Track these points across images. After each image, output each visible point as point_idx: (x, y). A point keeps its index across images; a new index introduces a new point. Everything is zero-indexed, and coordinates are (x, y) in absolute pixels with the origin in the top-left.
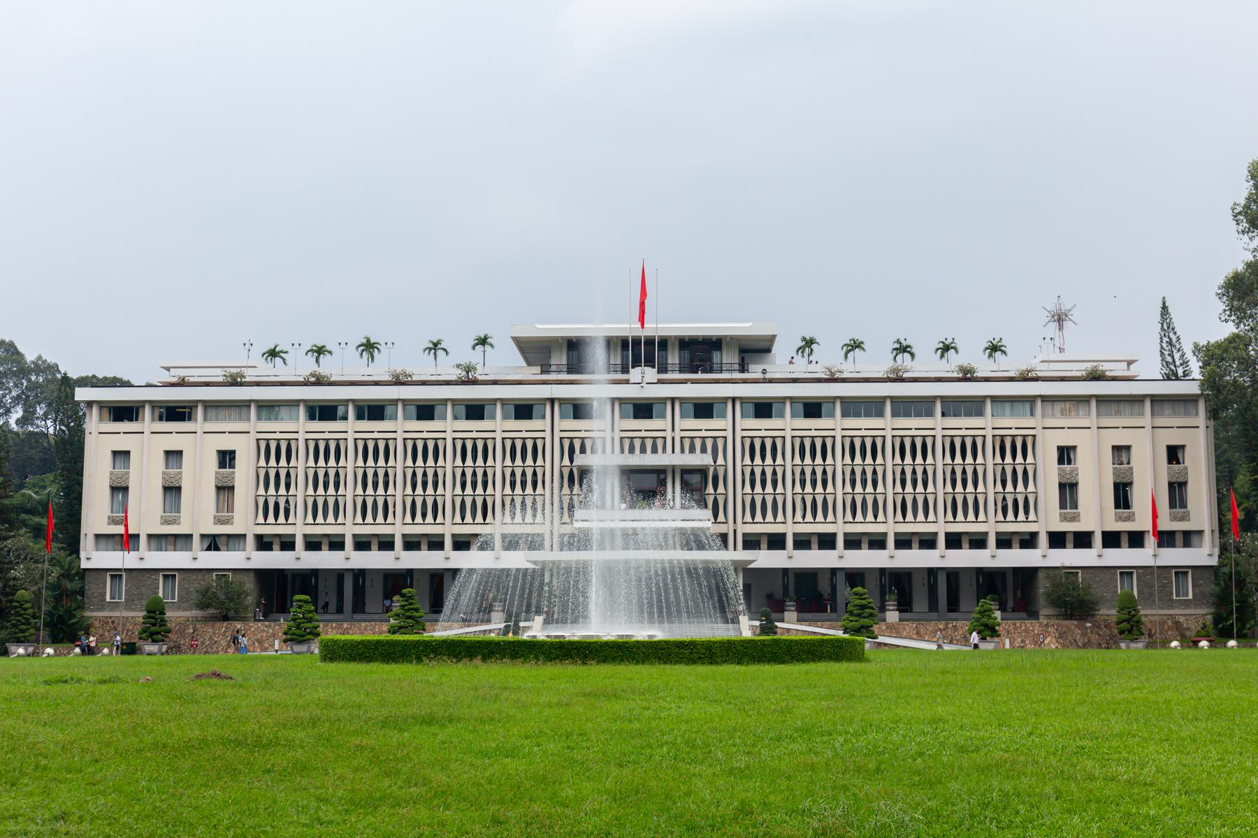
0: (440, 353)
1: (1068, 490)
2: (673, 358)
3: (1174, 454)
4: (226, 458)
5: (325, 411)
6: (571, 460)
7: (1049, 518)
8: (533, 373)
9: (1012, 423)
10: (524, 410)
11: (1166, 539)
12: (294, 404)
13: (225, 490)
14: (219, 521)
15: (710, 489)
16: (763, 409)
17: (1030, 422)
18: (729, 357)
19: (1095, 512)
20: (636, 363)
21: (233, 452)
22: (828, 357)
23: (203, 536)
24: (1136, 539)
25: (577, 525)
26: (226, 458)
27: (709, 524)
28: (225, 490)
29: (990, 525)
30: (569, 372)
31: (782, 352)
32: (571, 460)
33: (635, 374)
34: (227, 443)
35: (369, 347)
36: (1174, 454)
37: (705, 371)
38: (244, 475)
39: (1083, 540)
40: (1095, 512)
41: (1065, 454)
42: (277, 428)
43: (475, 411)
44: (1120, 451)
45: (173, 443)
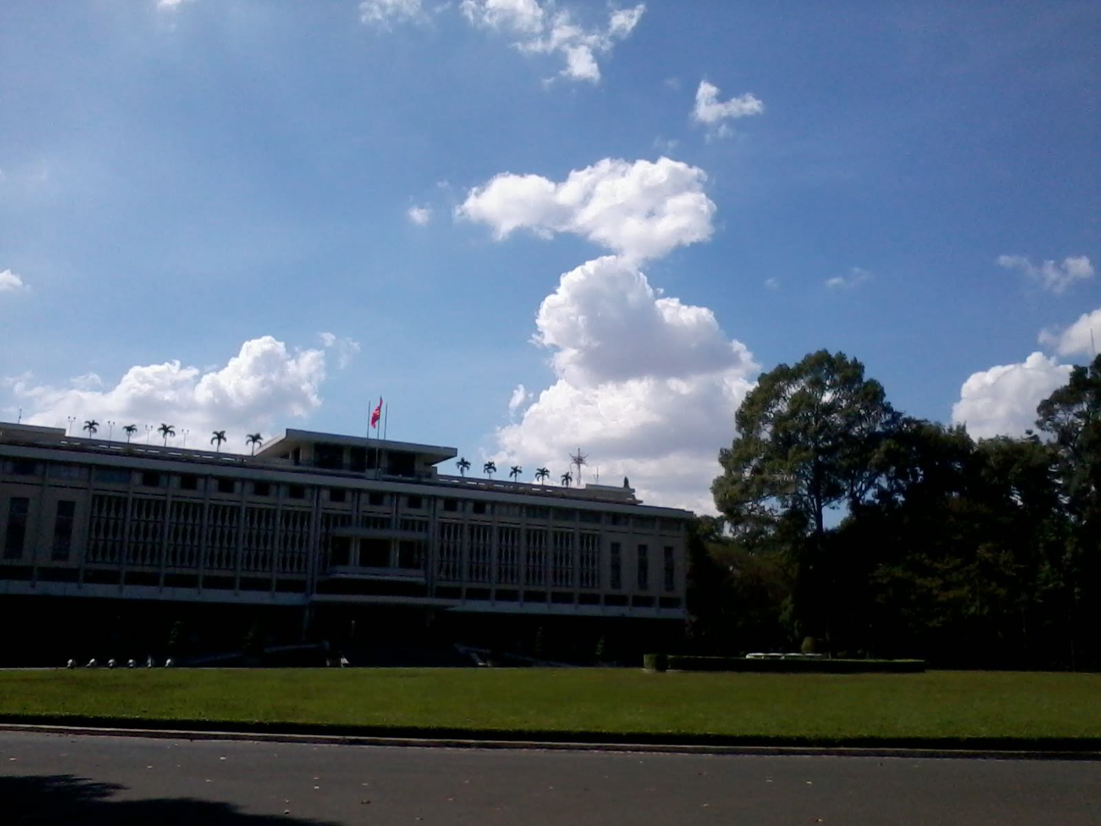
0: (222, 441)
1: (616, 567)
2: (385, 463)
3: (669, 551)
4: (66, 508)
5: (151, 478)
6: (327, 528)
7: (606, 588)
8: (288, 464)
9: (589, 527)
10: (296, 491)
11: (666, 603)
12: (130, 470)
13: (63, 530)
14: (56, 556)
15: (416, 556)
16: (451, 504)
17: (597, 526)
18: (418, 466)
19: (629, 586)
20: (371, 466)
21: (73, 503)
22: (476, 472)
23: (40, 569)
24: (646, 602)
25: (333, 576)
26: (66, 508)
27: (422, 580)
28: (63, 530)
29: (576, 589)
30: (315, 466)
31: (446, 468)
32: (327, 528)
33: (370, 473)
34: (67, 495)
35: (166, 429)
36: (669, 551)
37: (404, 475)
38: (79, 522)
39: (620, 601)
40: (629, 586)
41: (616, 547)
42: (113, 488)
43: (262, 488)
44: (643, 549)
45: (20, 492)
